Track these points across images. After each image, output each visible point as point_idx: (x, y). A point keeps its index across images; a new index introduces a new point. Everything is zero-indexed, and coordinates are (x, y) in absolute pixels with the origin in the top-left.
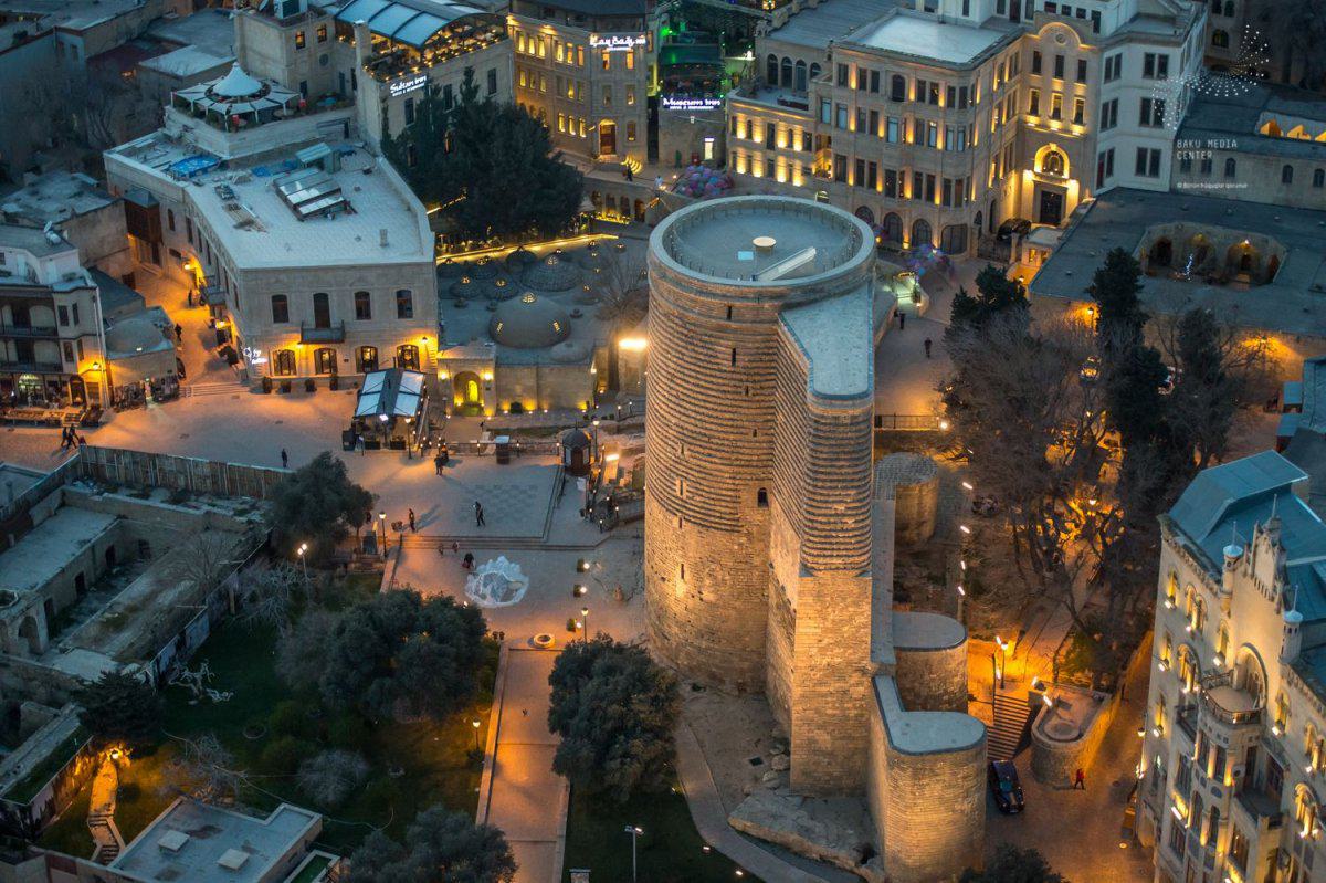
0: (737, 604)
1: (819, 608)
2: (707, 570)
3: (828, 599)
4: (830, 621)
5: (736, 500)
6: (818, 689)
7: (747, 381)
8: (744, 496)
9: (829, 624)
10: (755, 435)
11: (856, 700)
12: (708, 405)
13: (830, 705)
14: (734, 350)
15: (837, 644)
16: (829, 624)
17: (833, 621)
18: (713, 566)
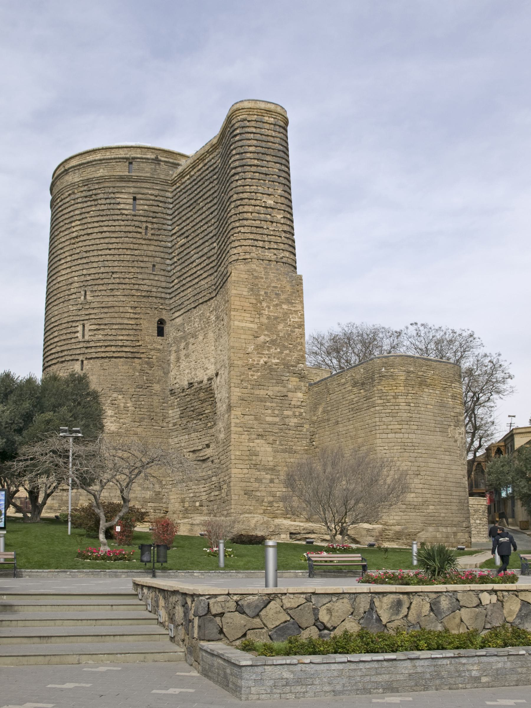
0: (139, 430)
1: (254, 301)
2: (109, 401)
3: (262, 293)
4: (265, 317)
5: (137, 329)
6: (257, 392)
7: (146, 222)
8: (145, 324)
9: (264, 320)
10: (153, 270)
11: (296, 407)
12: (110, 246)
13: (269, 411)
14: (135, 199)
15: (273, 342)
16: (264, 320)
17: (269, 318)
18: (115, 395)
